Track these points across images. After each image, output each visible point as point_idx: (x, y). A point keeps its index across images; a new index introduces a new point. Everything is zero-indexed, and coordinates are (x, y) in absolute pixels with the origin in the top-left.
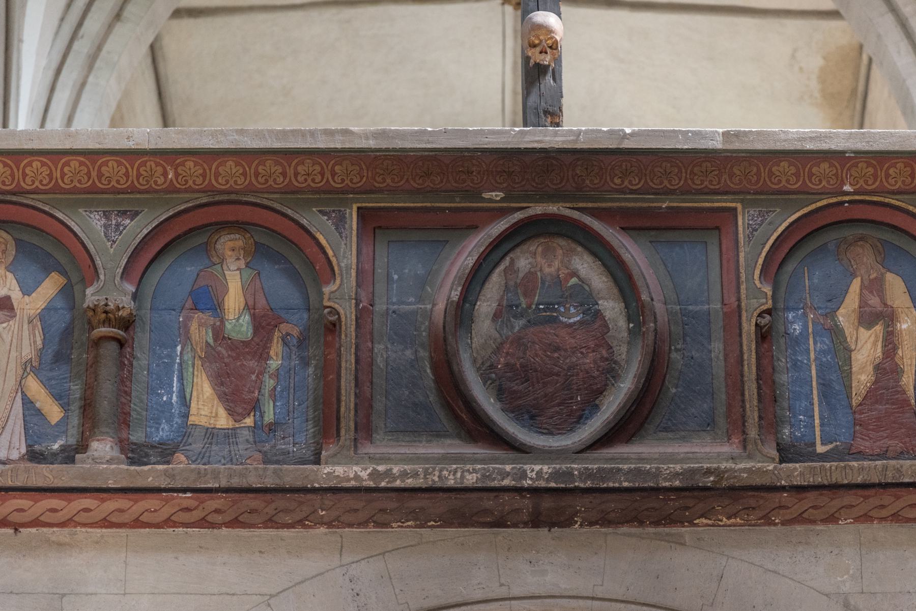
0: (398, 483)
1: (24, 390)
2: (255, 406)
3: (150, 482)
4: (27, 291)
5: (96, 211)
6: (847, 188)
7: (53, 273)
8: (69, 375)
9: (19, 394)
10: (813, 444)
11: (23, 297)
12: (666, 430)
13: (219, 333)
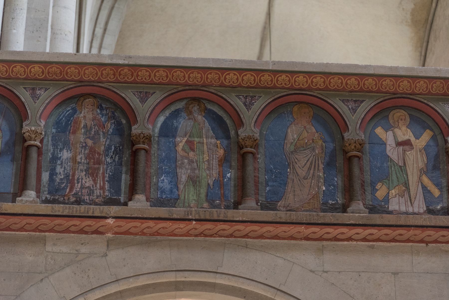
1: (422, 181)
4: (417, 138)
5: (447, 104)
7: (427, 130)
8: (440, 175)
9: (420, 183)
11: (416, 140)
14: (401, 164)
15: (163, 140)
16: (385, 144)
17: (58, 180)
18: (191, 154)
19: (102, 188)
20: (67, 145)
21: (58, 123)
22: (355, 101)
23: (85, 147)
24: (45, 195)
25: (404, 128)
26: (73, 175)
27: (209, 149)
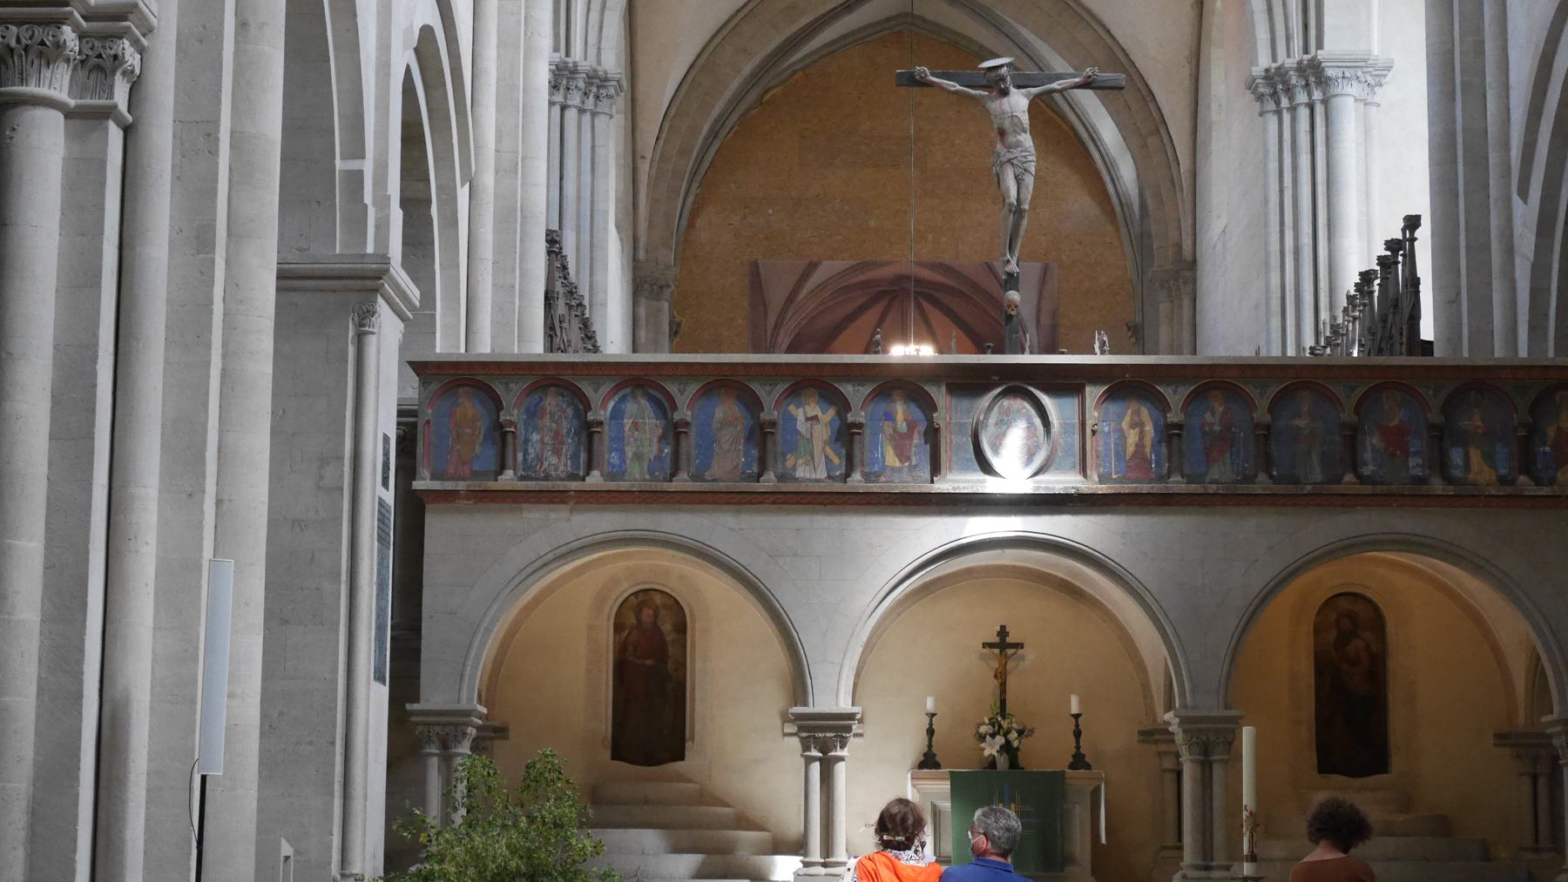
0: (962, 491)
2: (909, 459)
3: (875, 490)
6: (1127, 376)
10: (1111, 475)
12: (1057, 469)
13: (895, 430)
14: (809, 436)
15: (613, 422)
16: (796, 420)
17: (530, 460)
18: (636, 433)
19: (566, 465)
20: (536, 428)
21: (527, 411)
22: (771, 385)
23: (550, 430)
24: (521, 472)
25: (813, 405)
26: (542, 455)
27: (650, 429)
